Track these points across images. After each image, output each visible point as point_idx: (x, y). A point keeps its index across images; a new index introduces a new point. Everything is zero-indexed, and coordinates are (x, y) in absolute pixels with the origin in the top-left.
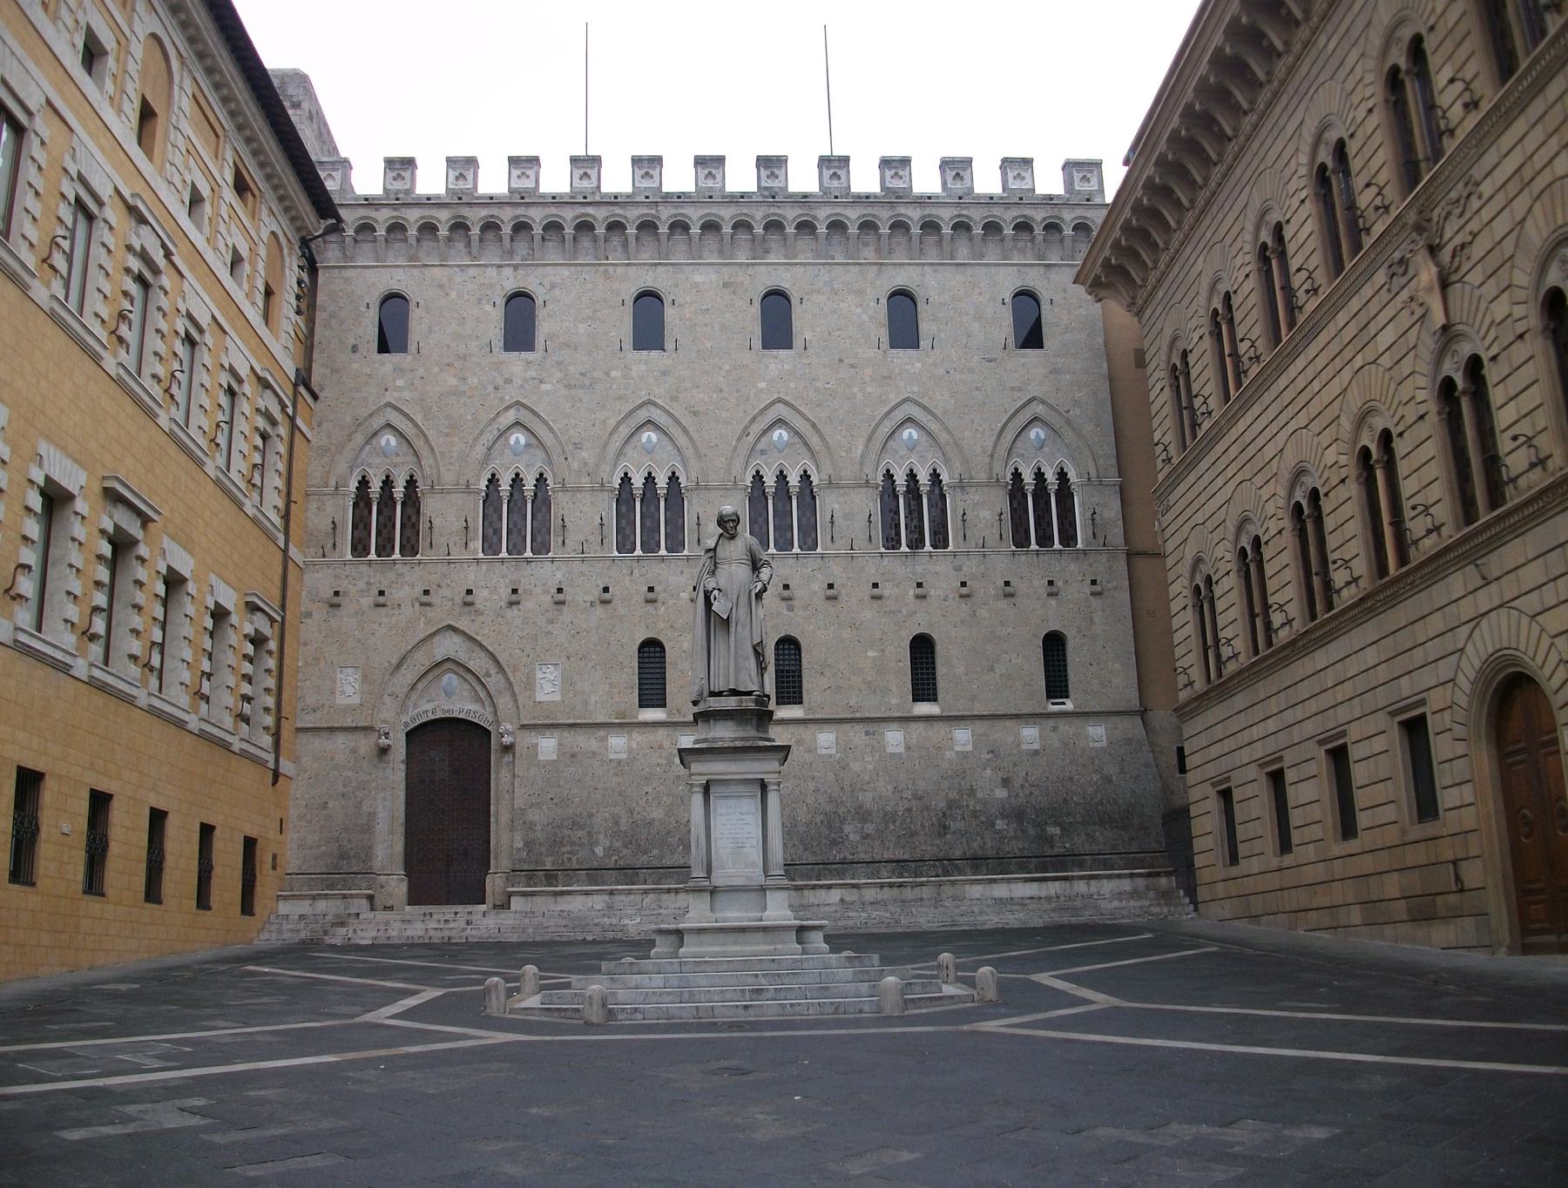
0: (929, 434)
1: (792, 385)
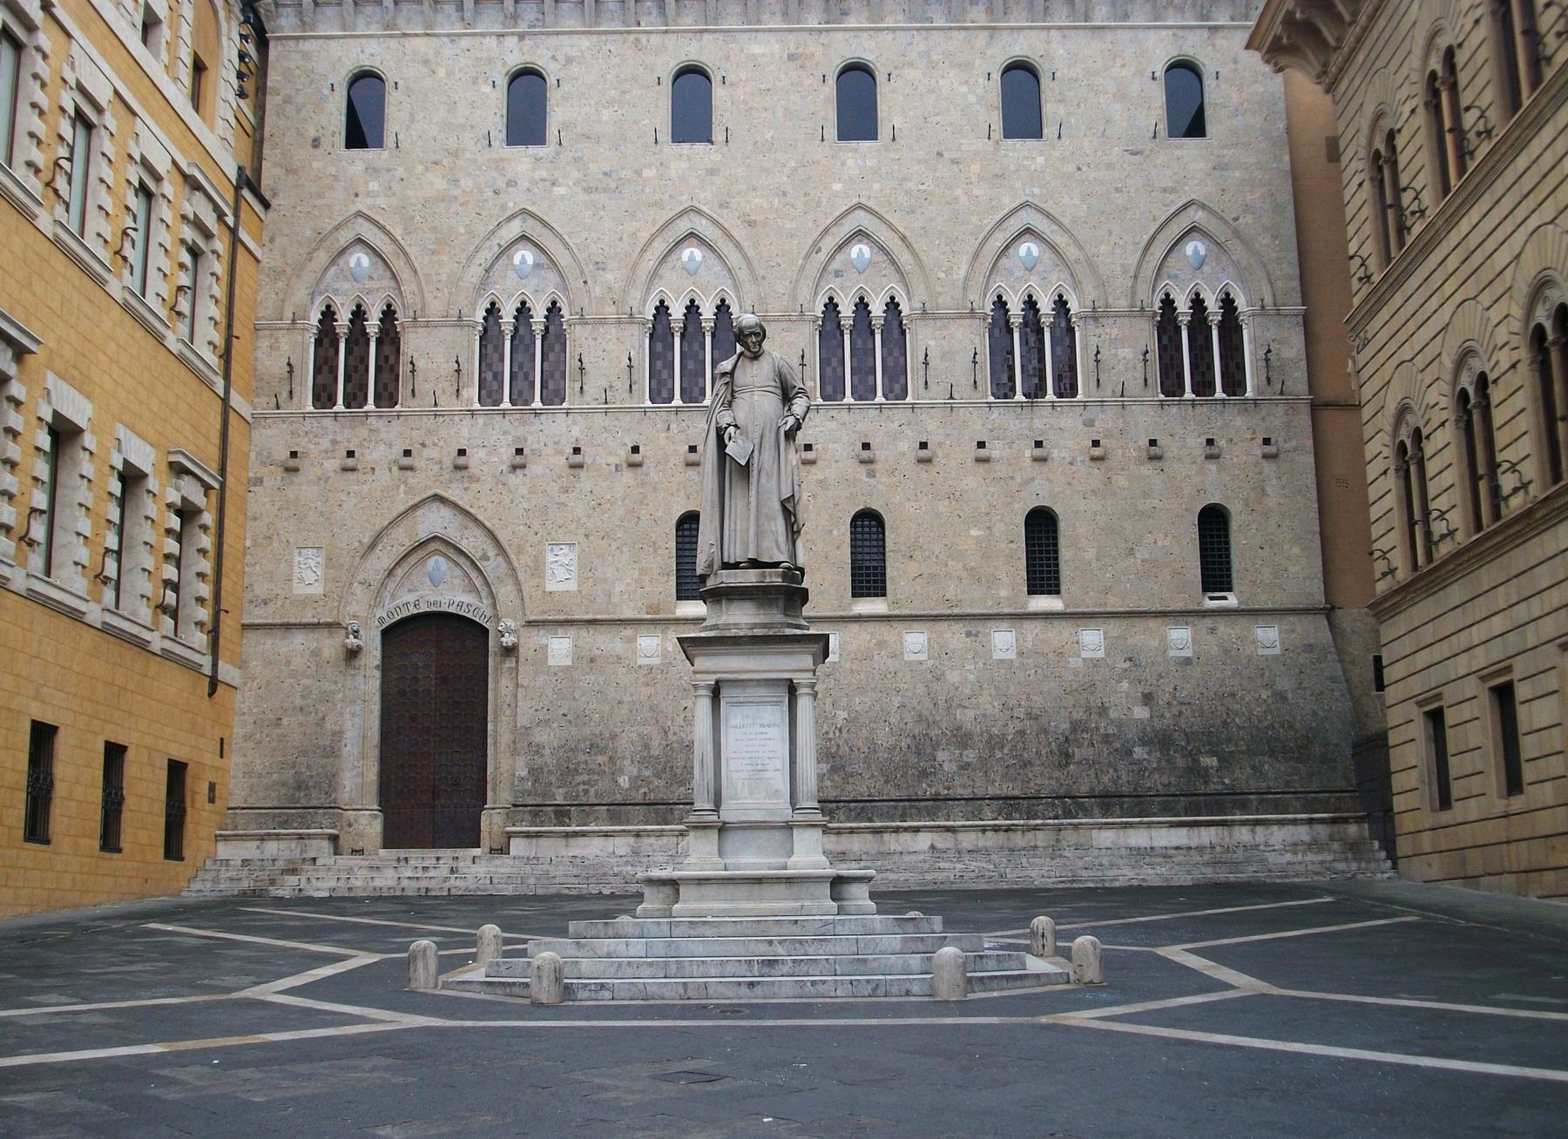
0: (1053, 248)
1: (876, 186)
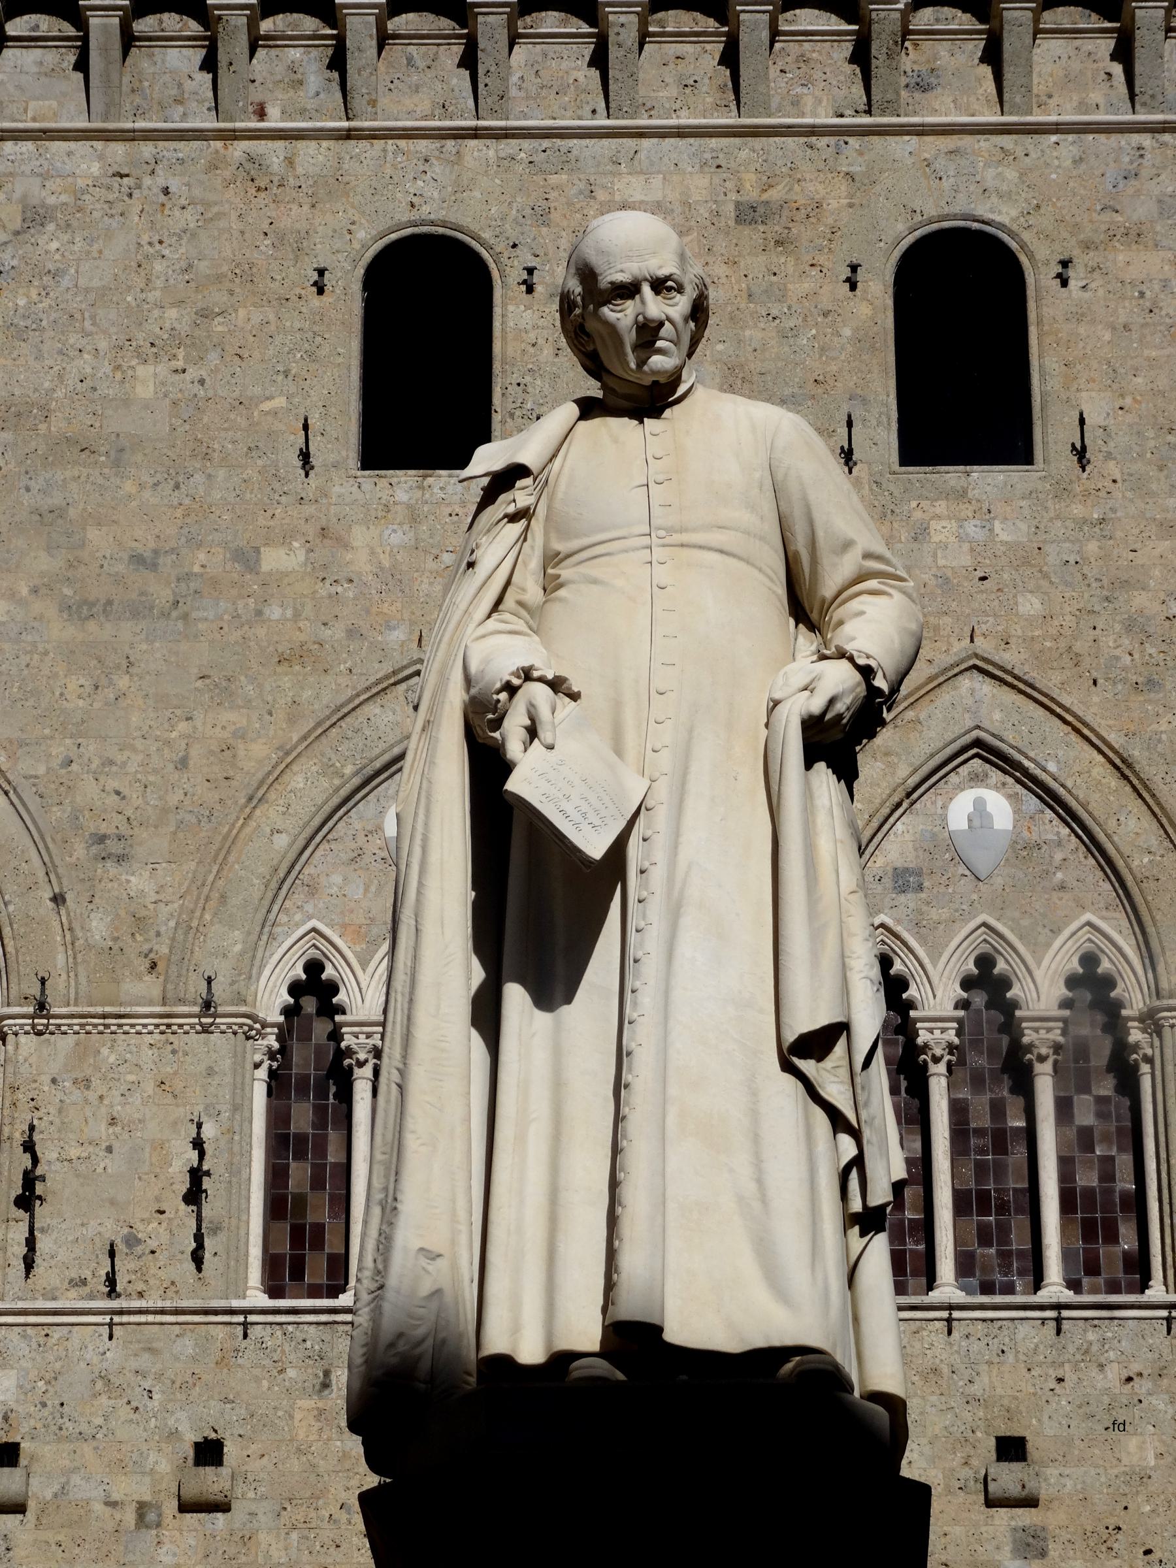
1: (1030, 605)
